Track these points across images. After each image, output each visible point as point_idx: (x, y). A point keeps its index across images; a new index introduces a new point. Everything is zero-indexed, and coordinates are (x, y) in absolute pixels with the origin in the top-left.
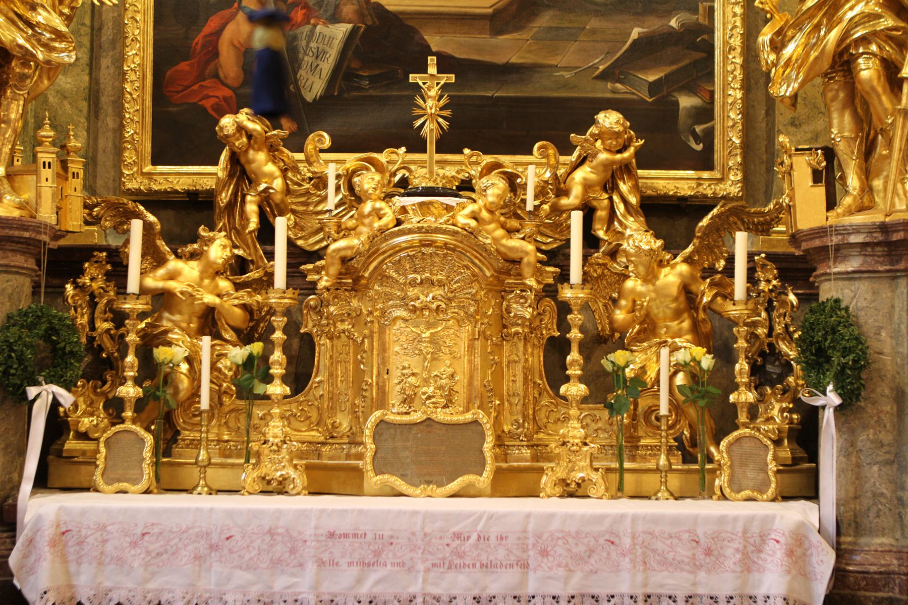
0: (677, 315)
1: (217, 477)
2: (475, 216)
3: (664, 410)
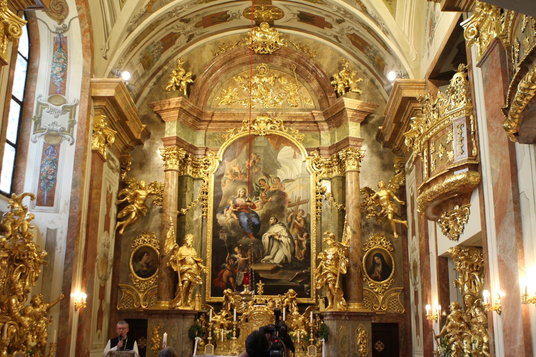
0: (302, 325)
1: (224, 353)
2: (267, 309)
3: (299, 342)
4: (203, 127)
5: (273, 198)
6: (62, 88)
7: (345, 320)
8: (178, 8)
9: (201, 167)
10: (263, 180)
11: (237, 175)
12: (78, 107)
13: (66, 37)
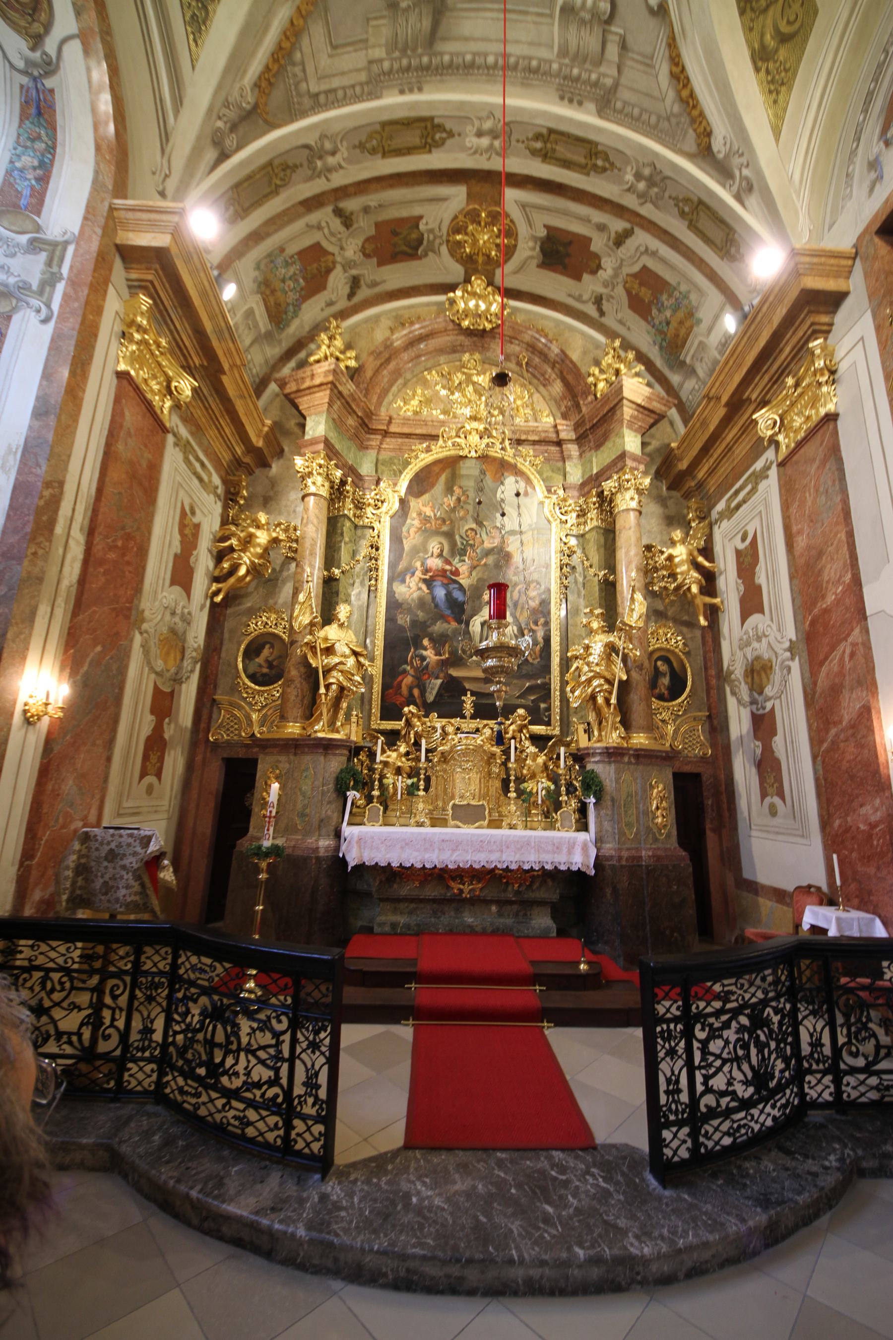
1: (402, 821)
4: (373, 443)
5: (490, 560)
6: (34, 201)
7: (630, 763)
8: (328, 146)
9: (369, 505)
10: (472, 529)
11: (429, 522)
12: (71, 249)
13: (52, 91)
